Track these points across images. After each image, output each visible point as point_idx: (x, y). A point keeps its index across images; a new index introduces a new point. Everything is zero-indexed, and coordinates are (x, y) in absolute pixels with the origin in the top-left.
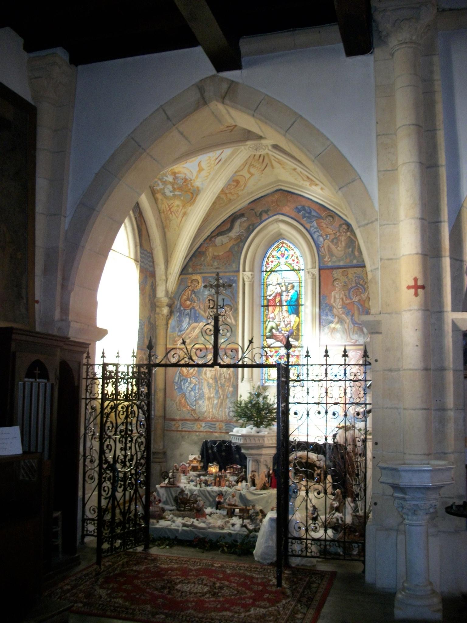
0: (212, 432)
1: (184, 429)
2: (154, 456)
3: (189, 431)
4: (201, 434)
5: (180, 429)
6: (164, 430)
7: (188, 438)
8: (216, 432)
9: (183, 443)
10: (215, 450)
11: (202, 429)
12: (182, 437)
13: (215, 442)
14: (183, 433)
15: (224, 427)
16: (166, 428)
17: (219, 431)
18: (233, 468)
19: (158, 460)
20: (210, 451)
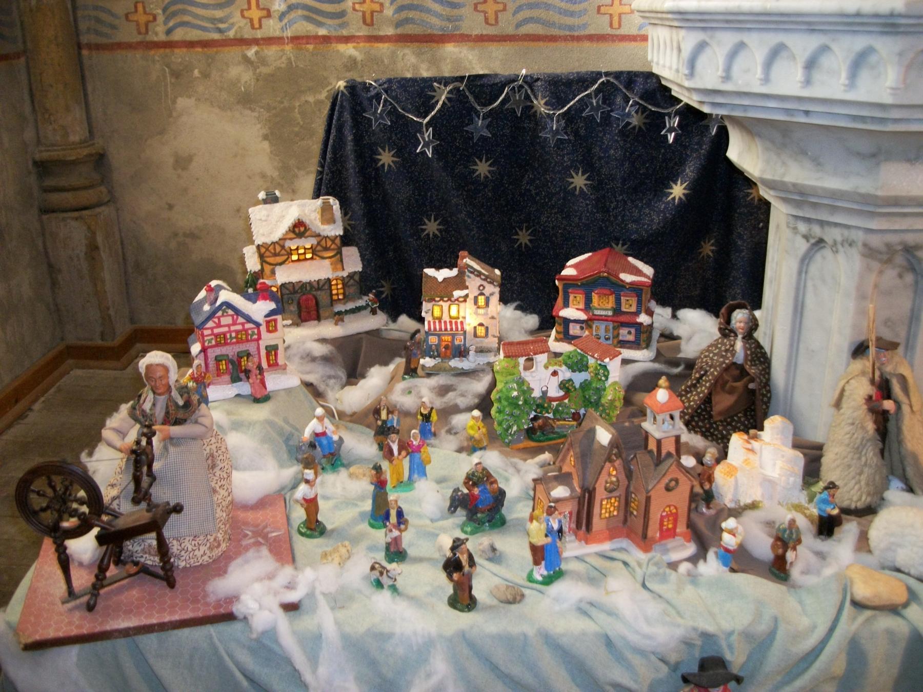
0: (326, 39)
1: (179, 35)
2: (50, 182)
3: (205, 44)
4: (271, 52)
5: (162, 37)
6: (79, 47)
7: (206, 75)
8: (347, 39)
9: (182, 102)
10: (426, 144)
11: (272, 27)
12: (176, 75)
13: (419, 92)
14: (179, 55)
15: (389, 11)
16: (84, 39)
17: (364, 31)
18: (617, 288)
19: (68, 198)
20: (386, 158)
